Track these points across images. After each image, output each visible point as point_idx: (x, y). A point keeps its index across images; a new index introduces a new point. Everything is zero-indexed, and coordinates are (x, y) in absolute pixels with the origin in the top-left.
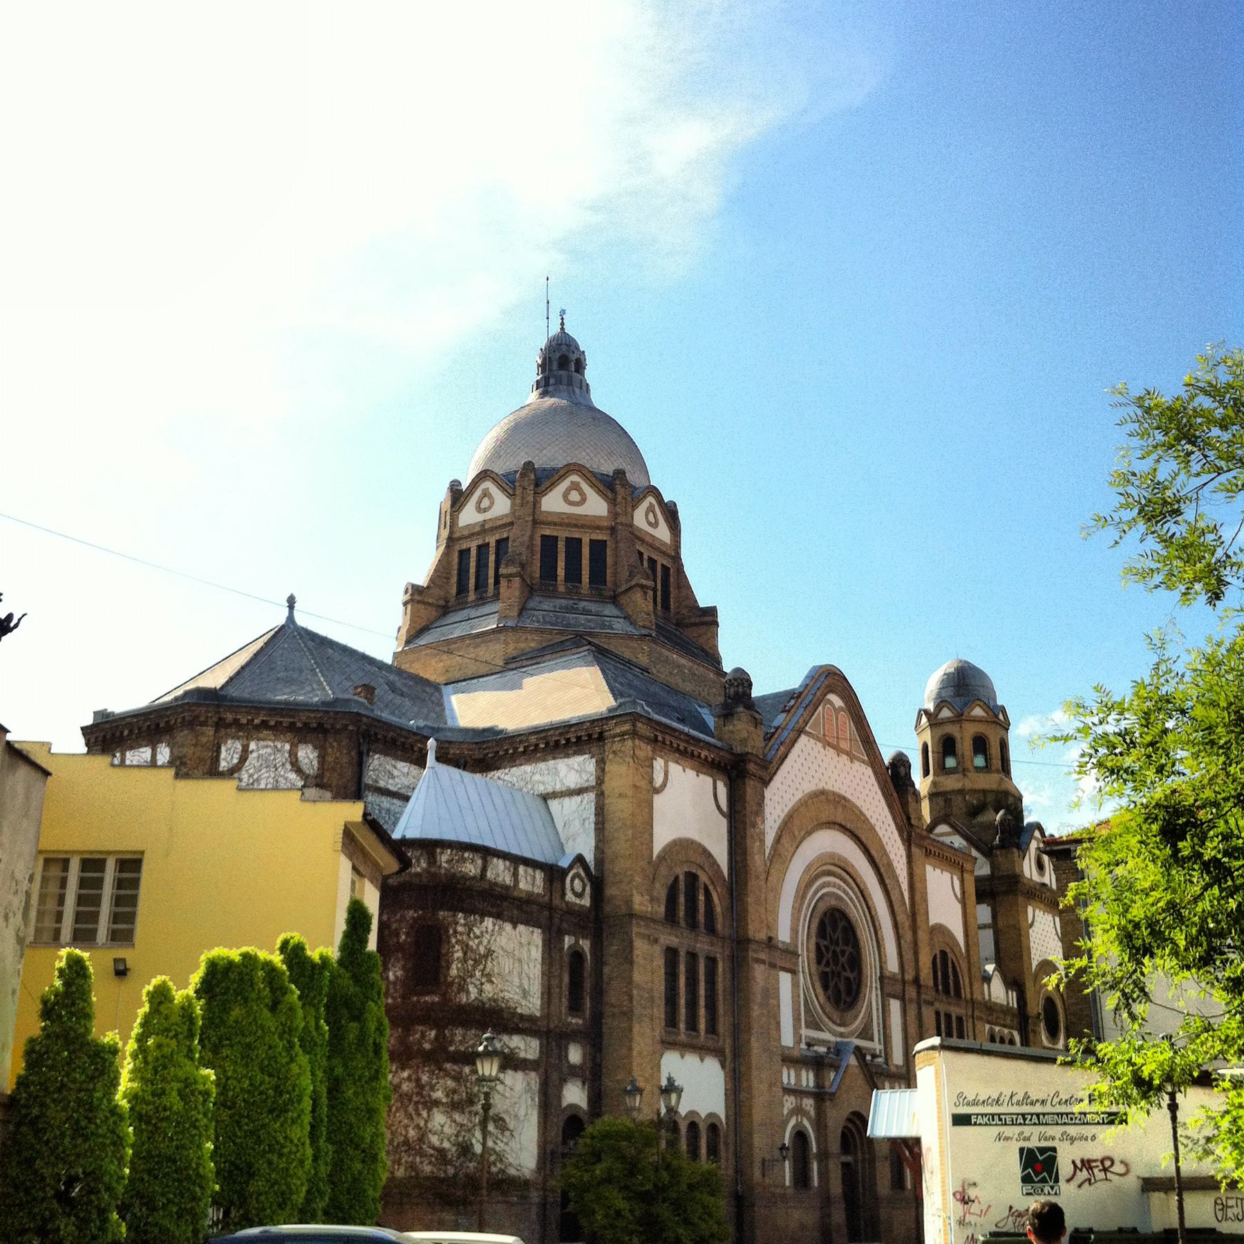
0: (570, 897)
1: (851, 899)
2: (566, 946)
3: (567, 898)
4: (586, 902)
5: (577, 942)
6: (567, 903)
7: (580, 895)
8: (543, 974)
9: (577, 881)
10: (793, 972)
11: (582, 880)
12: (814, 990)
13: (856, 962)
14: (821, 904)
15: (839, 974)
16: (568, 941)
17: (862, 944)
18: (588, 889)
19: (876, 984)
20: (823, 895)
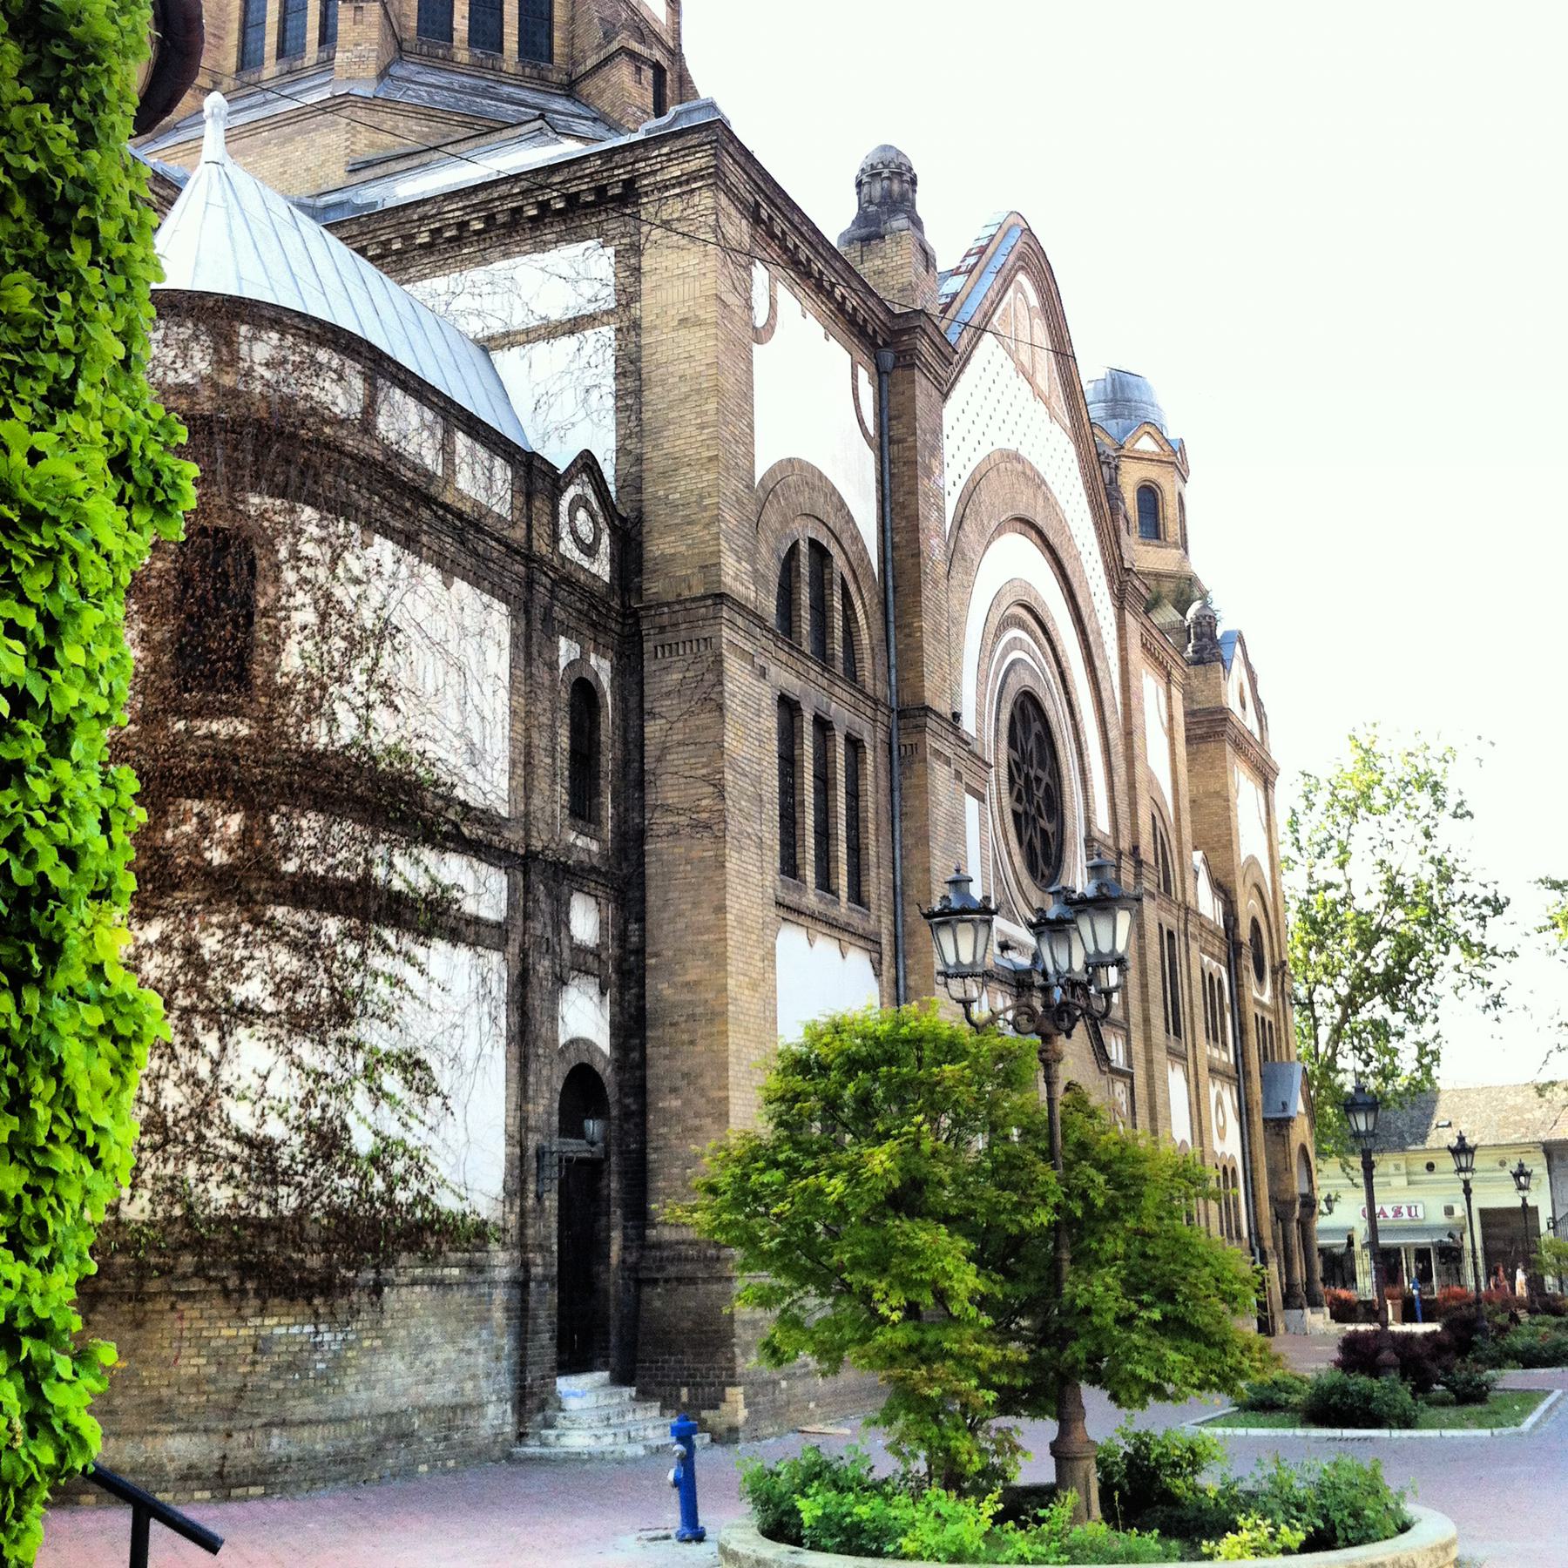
0: (567, 546)
1: (1048, 682)
2: (563, 663)
3: (562, 547)
4: (602, 568)
5: (583, 658)
6: (563, 557)
7: (590, 550)
8: (513, 712)
9: (582, 515)
10: (981, 798)
11: (592, 516)
12: (1007, 845)
13: (1054, 804)
14: (1012, 679)
15: (1034, 819)
16: (566, 650)
17: (1064, 772)
18: (605, 540)
19: (1081, 851)
20: (1013, 663)
